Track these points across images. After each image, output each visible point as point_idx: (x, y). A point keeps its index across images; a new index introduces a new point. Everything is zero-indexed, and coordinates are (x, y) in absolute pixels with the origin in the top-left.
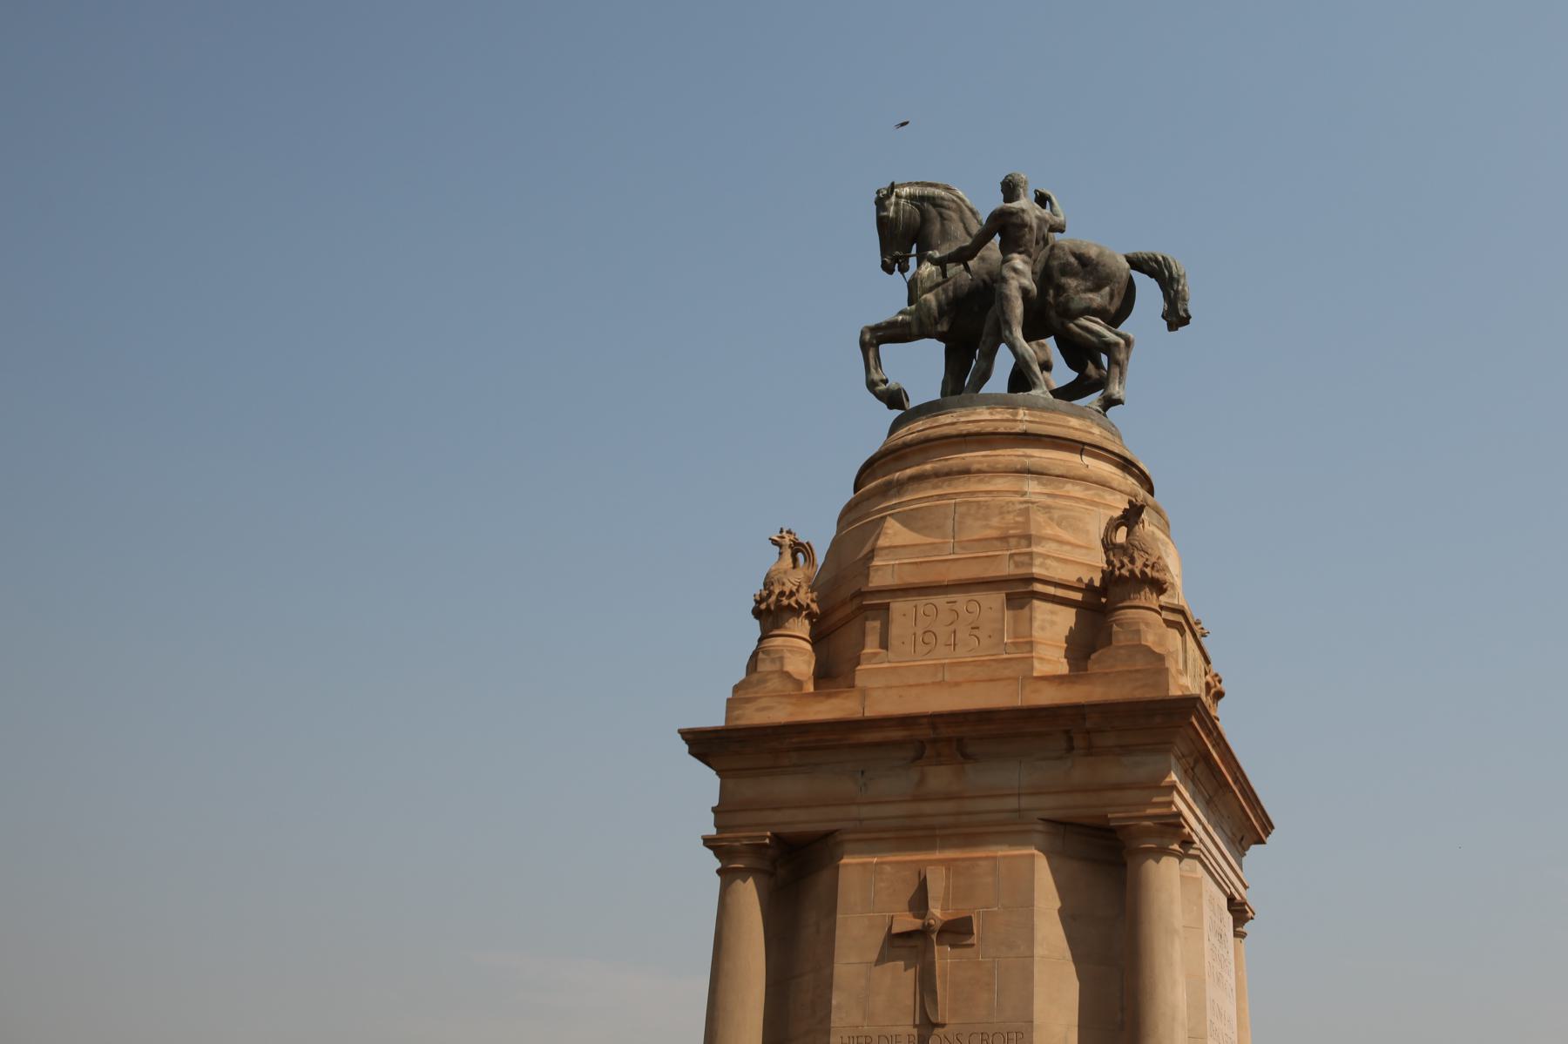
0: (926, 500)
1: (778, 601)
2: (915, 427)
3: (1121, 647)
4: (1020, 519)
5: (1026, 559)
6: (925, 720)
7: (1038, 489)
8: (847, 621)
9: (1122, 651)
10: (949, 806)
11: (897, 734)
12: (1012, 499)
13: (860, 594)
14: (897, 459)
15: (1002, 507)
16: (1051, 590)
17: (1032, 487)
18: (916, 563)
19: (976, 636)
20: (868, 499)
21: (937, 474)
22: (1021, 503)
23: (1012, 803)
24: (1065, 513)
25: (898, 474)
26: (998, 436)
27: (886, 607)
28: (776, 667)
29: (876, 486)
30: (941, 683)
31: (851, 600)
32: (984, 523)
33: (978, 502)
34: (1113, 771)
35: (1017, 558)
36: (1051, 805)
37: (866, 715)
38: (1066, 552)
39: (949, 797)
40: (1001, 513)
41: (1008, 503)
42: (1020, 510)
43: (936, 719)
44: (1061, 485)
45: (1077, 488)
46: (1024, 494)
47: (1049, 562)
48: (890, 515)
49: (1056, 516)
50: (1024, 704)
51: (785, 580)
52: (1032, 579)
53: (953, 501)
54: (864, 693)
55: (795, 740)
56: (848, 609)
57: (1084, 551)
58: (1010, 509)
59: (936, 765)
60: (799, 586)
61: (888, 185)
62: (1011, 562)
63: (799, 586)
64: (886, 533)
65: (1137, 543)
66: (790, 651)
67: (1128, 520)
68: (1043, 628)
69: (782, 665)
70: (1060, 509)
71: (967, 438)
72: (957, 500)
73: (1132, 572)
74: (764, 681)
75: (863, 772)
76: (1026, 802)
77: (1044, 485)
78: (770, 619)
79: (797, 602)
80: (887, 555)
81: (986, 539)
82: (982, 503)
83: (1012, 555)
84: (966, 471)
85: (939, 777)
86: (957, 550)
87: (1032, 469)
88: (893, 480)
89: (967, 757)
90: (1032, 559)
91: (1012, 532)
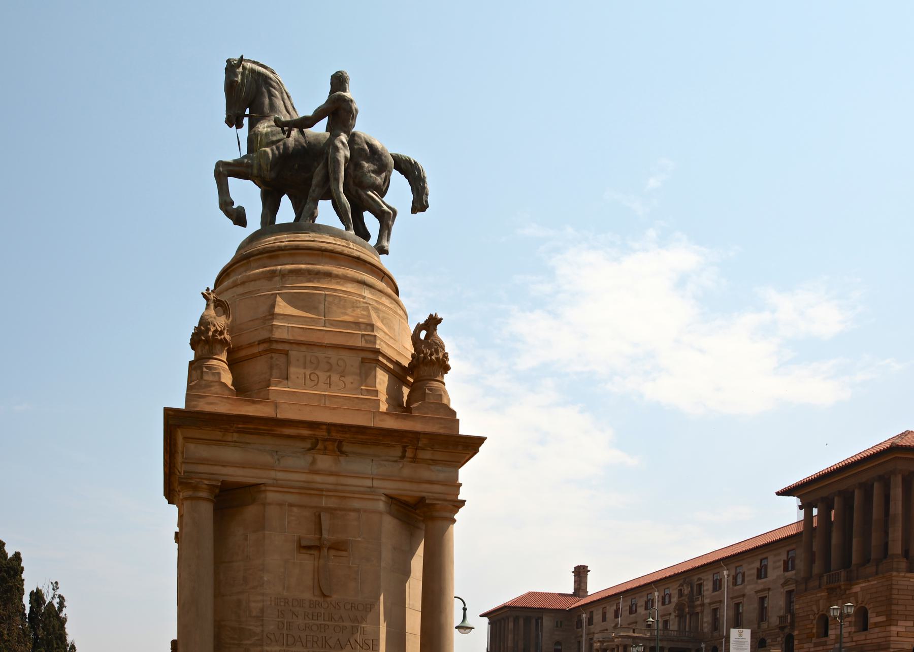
0: (304, 288)
1: (214, 335)
2: (282, 238)
3: (433, 403)
4: (365, 313)
5: (372, 338)
6: (324, 427)
7: (369, 296)
8: (254, 356)
9: (432, 406)
10: (331, 479)
11: (305, 432)
12: (360, 299)
13: (269, 341)
14: (270, 257)
15: (353, 303)
16: (385, 362)
17: (367, 293)
18: (303, 328)
19: (343, 381)
20: (255, 280)
21: (309, 272)
22: (364, 302)
23: (368, 483)
24: (385, 315)
25: (279, 267)
26: (343, 256)
27: (287, 354)
28: (216, 379)
29: (262, 272)
30: (324, 407)
31: (259, 344)
32: (343, 311)
33: (339, 296)
34: (426, 473)
35: (366, 337)
36: (391, 487)
37: (278, 417)
38: (386, 339)
39: (331, 474)
40: (353, 307)
41: (357, 301)
42: (363, 307)
43: (331, 427)
44: (380, 297)
45: (387, 301)
46: (364, 297)
47: (382, 343)
48: (279, 294)
49: (381, 316)
50: (375, 426)
51: (216, 323)
52: (378, 352)
53: (324, 292)
54: (276, 405)
55: (240, 426)
56: (256, 350)
57: (393, 341)
58: (358, 305)
59: (323, 454)
60: (224, 329)
61: (238, 57)
62: (363, 339)
63: (224, 329)
64: (279, 305)
65: (438, 342)
66: (223, 370)
67: (429, 327)
68: (380, 384)
69: (220, 377)
70: (383, 312)
71: (324, 253)
72: (326, 293)
73: (437, 359)
74: (210, 386)
75: (276, 452)
76: (376, 483)
77: (373, 295)
78: (207, 347)
79: (224, 338)
80: (282, 319)
81: (346, 322)
82: (342, 298)
83: (363, 335)
84: (328, 275)
85: (325, 462)
86: (327, 325)
87: (367, 282)
88: (276, 270)
89: (342, 453)
90: (376, 339)
91: (361, 320)
